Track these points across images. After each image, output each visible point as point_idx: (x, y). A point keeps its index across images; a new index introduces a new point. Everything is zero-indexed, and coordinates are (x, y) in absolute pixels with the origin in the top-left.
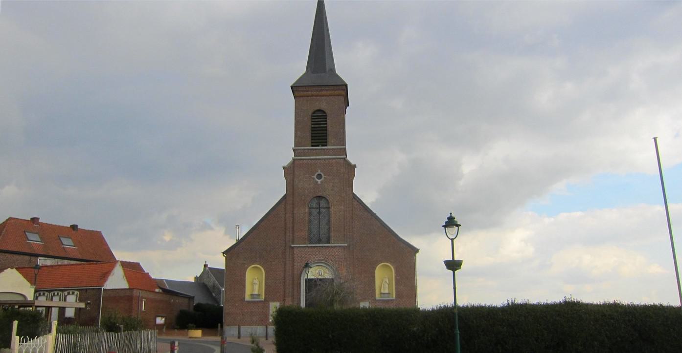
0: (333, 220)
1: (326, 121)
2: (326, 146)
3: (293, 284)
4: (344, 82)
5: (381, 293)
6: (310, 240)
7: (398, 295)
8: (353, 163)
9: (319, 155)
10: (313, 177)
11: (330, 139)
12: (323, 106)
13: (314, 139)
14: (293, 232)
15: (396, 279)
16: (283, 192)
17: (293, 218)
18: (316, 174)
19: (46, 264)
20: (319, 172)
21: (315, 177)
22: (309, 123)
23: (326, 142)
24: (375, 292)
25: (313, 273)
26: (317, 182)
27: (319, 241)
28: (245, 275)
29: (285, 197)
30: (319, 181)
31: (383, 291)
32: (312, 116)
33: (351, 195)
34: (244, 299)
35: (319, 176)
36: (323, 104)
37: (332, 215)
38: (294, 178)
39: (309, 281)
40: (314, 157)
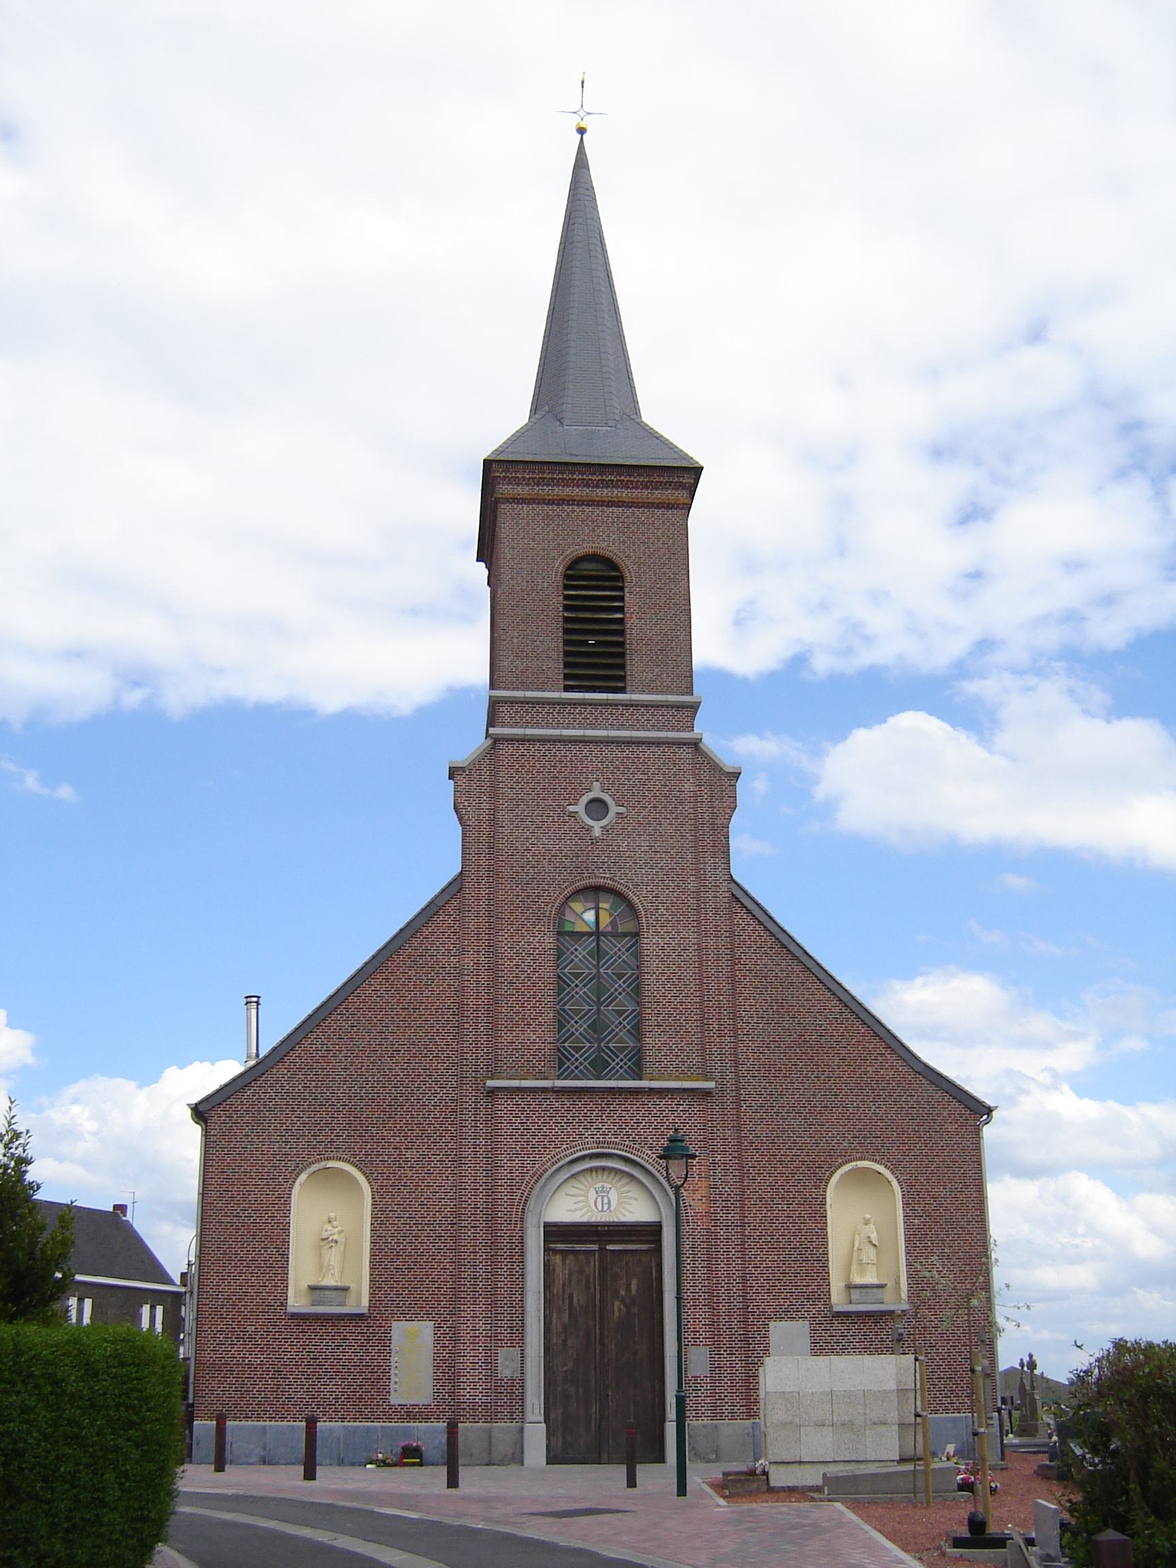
0: (653, 984)
1: (622, 599)
2: (622, 690)
3: (494, 1244)
4: (686, 457)
5: (850, 1287)
6: (561, 1064)
7: (914, 1293)
8: (728, 763)
9: (593, 721)
10: (571, 808)
11: (635, 666)
12: (608, 543)
13: (611, 655)
14: (493, 1025)
15: (908, 1227)
16: (445, 863)
17: (494, 969)
18: (585, 800)
19: (636, 658)
20: (596, 792)
21: (580, 808)
22: (557, 602)
23: (623, 678)
24: (826, 1279)
25: (576, 1202)
26: (589, 829)
27: (599, 1067)
28: (287, 1203)
29: (456, 888)
30: (597, 827)
31: (858, 1280)
32: (567, 577)
33: (724, 886)
34: (284, 1304)
35: (597, 807)
36: (604, 533)
37: (652, 965)
38: (495, 810)
39: (556, 1233)
40: (579, 732)
